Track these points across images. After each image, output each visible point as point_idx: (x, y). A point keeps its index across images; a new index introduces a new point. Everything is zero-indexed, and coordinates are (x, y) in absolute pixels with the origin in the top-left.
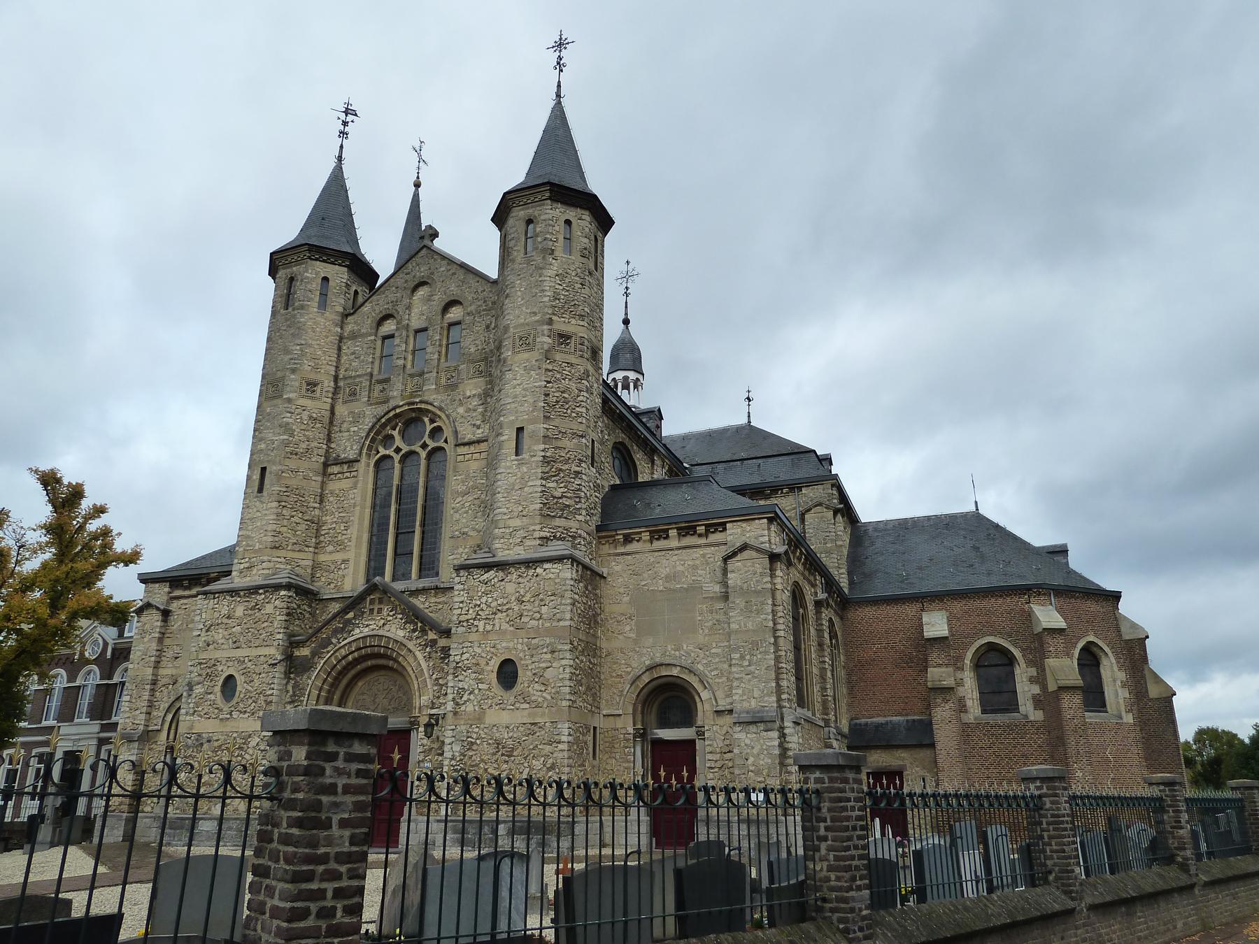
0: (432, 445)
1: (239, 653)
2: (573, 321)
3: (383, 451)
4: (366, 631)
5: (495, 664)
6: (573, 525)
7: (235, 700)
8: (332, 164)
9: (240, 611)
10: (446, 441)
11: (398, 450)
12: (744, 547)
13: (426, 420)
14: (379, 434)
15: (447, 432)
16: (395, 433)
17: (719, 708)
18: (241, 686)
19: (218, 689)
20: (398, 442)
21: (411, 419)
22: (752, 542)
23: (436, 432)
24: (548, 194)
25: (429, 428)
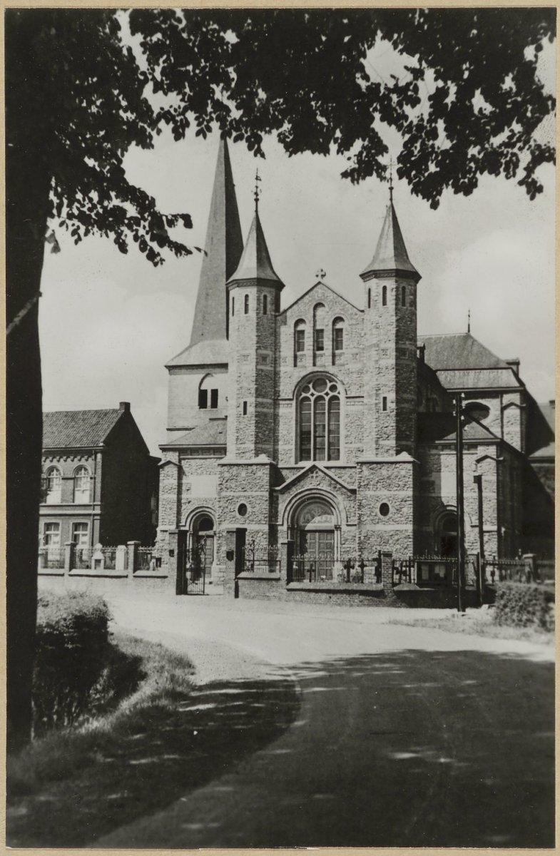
0: (331, 394)
1: (246, 494)
2: (407, 343)
3: (304, 395)
4: (311, 487)
5: (379, 505)
6: (409, 443)
7: (247, 515)
8: (254, 214)
9: (243, 474)
10: (339, 393)
11: (312, 395)
12: (486, 457)
13: (328, 381)
14: (302, 386)
15: (340, 388)
16: (311, 386)
17: (473, 524)
18: (249, 509)
19: (237, 510)
20: (312, 391)
21: (319, 379)
22: (489, 455)
23: (333, 388)
24: (394, 274)
25: (329, 385)
